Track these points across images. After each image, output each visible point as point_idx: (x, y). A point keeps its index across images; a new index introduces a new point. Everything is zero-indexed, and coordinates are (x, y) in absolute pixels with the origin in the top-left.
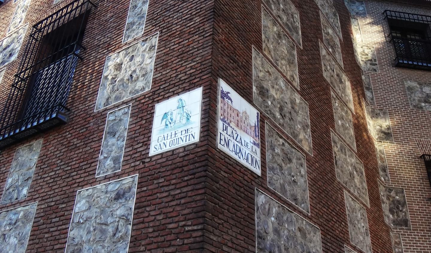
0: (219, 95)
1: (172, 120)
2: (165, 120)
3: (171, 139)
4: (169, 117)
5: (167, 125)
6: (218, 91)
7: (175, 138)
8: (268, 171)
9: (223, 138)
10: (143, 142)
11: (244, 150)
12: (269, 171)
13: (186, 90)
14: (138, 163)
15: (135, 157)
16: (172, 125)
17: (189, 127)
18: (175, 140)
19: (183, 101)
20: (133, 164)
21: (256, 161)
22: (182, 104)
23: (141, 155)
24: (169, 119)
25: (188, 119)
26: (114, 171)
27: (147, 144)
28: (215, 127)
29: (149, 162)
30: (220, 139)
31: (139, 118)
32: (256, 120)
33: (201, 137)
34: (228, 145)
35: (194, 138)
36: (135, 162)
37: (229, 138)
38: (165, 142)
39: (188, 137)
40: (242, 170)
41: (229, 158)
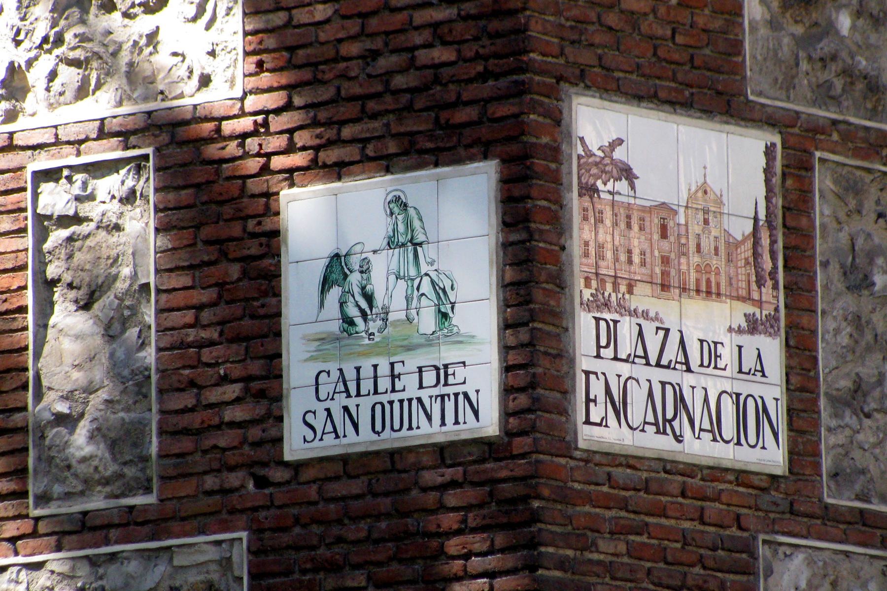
0: (570, 190)
1: (369, 298)
2: (335, 293)
3: (378, 398)
4: (355, 278)
5: (349, 321)
6: (564, 169)
7: (396, 397)
8: (826, 416)
9: (597, 389)
10: (247, 379)
11: (703, 386)
12: (836, 415)
13: (422, 152)
14: (234, 479)
15: (215, 447)
16: (374, 326)
17: (448, 354)
18: (396, 406)
19: (411, 211)
20: (210, 482)
21: (763, 411)
22: (408, 224)
23: (242, 444)
24: (357, 290)
25: (445, 316)
26: (123, 495)
27: (266, 385)
28: (563, 356)
29: (288, 482)
30: (588, 400)
31: (208, 243)
32: (762, 191)
33: (506, 414)
34: (620, 409)
35: (476, 413)
36: (219, 471)
37: (625, 369)
38: (351, 403)
39: (450, 405)
40: (695, 482)
41: (631, 462)
